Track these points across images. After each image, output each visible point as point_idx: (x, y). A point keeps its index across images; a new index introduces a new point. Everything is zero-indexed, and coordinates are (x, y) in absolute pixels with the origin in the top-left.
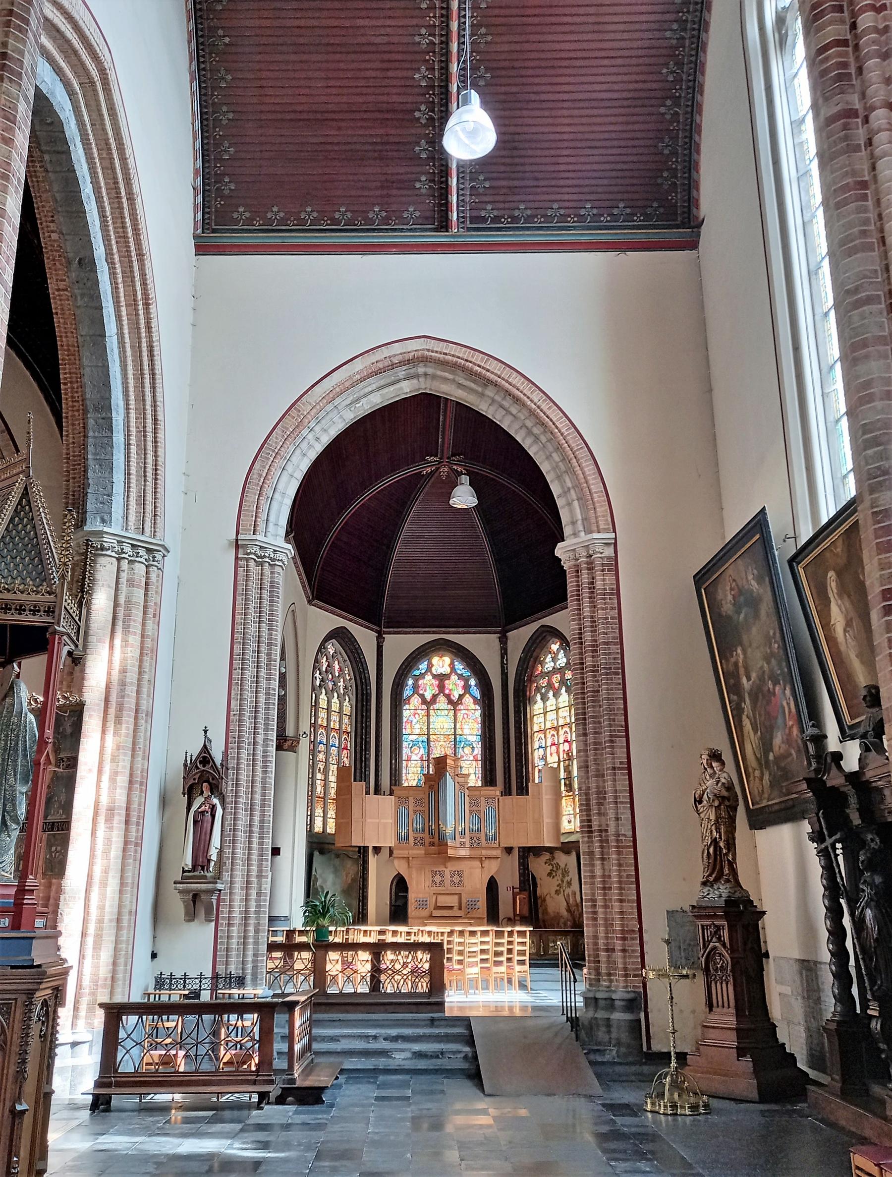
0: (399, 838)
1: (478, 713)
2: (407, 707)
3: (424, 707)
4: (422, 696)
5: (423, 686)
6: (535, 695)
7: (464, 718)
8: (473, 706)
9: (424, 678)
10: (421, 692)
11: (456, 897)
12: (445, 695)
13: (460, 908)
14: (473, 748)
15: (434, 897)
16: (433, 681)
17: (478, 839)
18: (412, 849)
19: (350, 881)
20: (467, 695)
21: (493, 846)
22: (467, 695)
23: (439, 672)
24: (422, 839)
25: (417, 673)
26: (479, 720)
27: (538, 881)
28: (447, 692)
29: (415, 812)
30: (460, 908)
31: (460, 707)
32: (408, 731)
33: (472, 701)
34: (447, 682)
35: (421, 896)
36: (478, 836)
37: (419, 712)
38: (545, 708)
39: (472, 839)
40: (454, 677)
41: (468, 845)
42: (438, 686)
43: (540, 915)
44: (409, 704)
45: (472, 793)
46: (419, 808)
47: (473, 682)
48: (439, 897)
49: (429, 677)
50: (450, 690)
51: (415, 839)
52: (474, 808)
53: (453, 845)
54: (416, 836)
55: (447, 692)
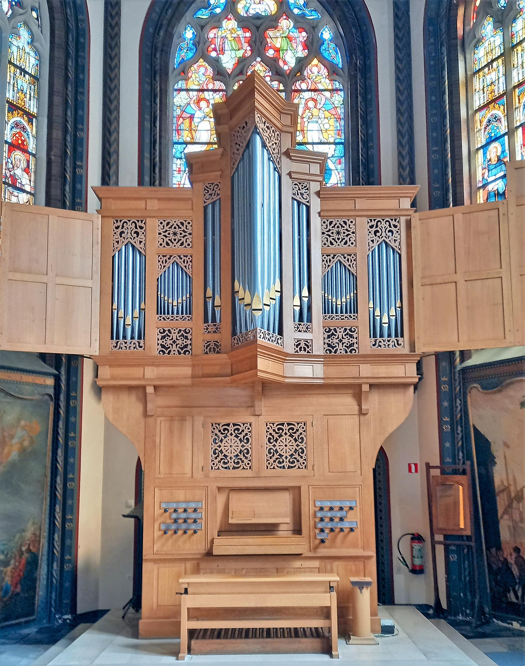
0: (114, 335)
1: (339, 98)
2: (181, 84)
3: (219, 85)
4: (216, 64)
5: (218, 41)
6: (478, 24)
7: (307, 108)
8: (325, 83)
9: (218, 27)
10: (214, 54)
11: (286, 498)
12: (266, 61)
13: (297, 531)
14: (325, 171)
15: (221, 500)
16: (240, 32)
17: (350, 333)
18: (154, 363)
19: (14, 455)
20: (315, 61)
21: (392, 350)
22: (315, 61)
23: (252, 12)
24: (185, 334)
25: (204, 14)
26: (341, 111)
27: (497, 450)
28: (271, 53)
29: (165, 258)
30: (297, 531)
31: (298, 85)
32: (186, 136)
33: (324, 72)
34: (270, 33)
35: (180, 495)
36: (349, 323)
37: (206, 95)
38: (508, 38)
39: (330, 333)
40: (285, 24)
41: (318, 348)
42: (251, 42)
43: (505, 534)
44: (187, 79)
45: (332, 205)
46: (176, 249)
47: (327, 34)
48: (234, 497)
49: (230, 24)
50: (277, 50)
51: (165, 334)
52: (339, 247)
53: (273, 345)
54: (166, 325)
55: (271, 53)
